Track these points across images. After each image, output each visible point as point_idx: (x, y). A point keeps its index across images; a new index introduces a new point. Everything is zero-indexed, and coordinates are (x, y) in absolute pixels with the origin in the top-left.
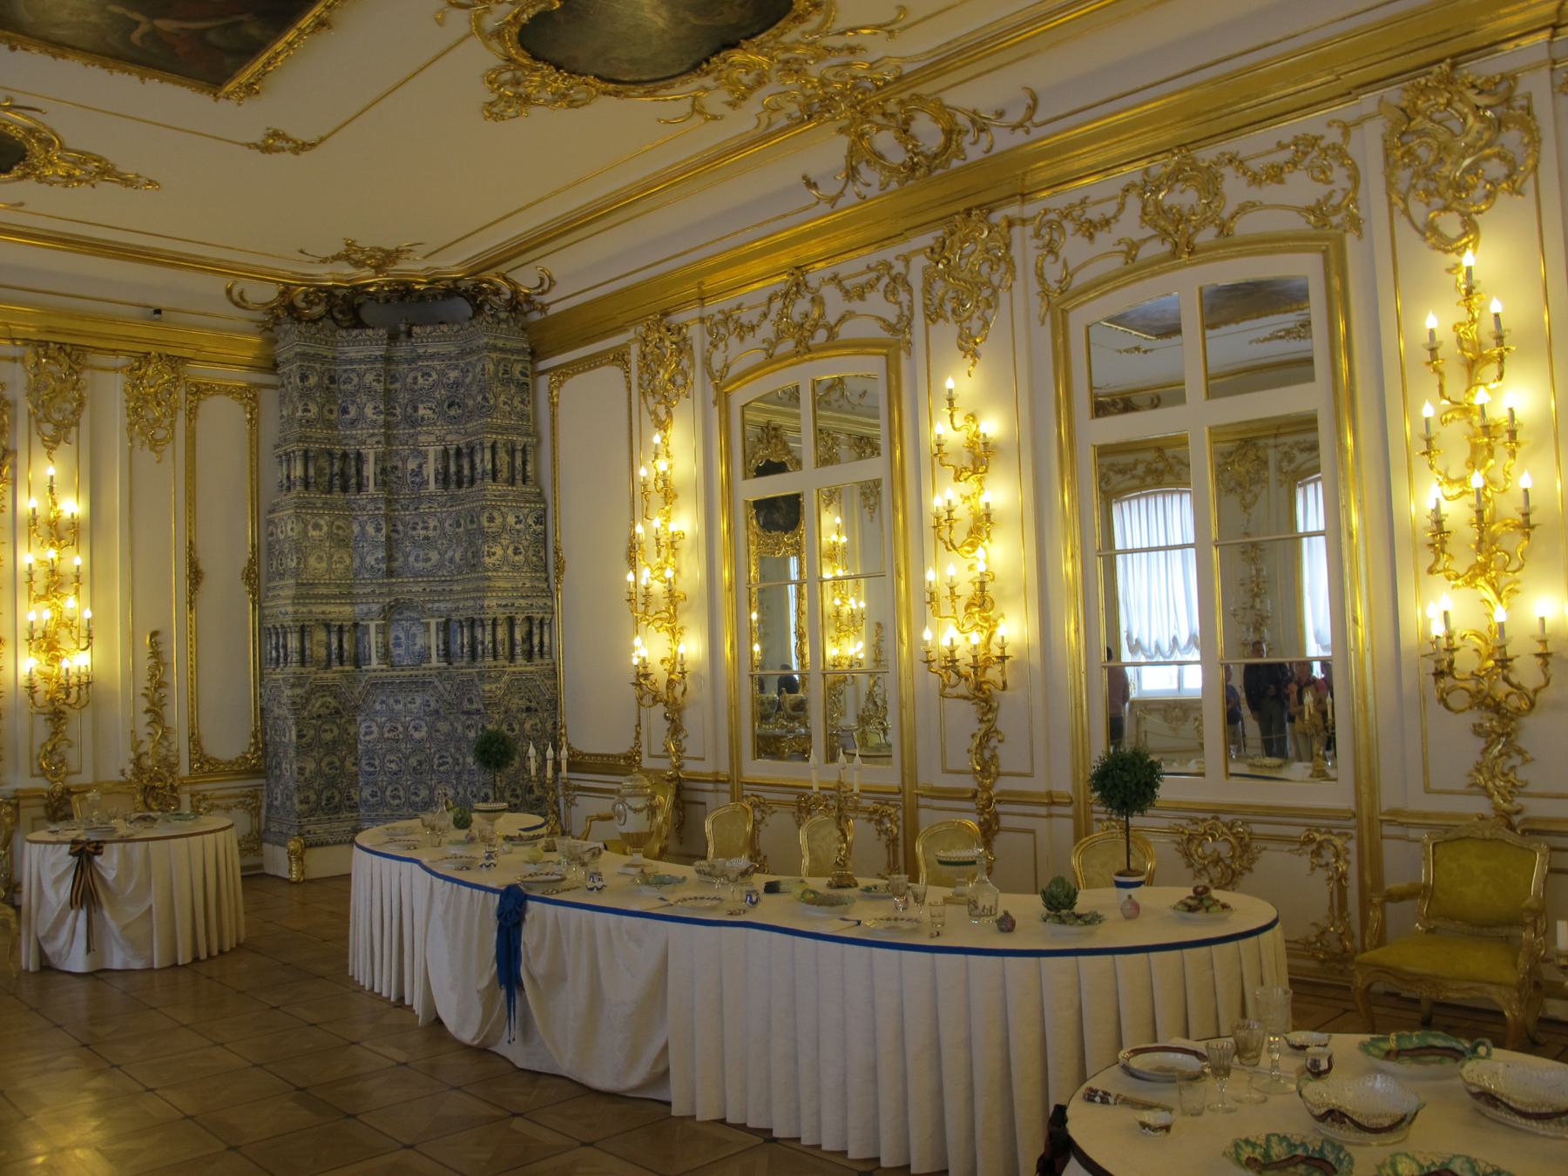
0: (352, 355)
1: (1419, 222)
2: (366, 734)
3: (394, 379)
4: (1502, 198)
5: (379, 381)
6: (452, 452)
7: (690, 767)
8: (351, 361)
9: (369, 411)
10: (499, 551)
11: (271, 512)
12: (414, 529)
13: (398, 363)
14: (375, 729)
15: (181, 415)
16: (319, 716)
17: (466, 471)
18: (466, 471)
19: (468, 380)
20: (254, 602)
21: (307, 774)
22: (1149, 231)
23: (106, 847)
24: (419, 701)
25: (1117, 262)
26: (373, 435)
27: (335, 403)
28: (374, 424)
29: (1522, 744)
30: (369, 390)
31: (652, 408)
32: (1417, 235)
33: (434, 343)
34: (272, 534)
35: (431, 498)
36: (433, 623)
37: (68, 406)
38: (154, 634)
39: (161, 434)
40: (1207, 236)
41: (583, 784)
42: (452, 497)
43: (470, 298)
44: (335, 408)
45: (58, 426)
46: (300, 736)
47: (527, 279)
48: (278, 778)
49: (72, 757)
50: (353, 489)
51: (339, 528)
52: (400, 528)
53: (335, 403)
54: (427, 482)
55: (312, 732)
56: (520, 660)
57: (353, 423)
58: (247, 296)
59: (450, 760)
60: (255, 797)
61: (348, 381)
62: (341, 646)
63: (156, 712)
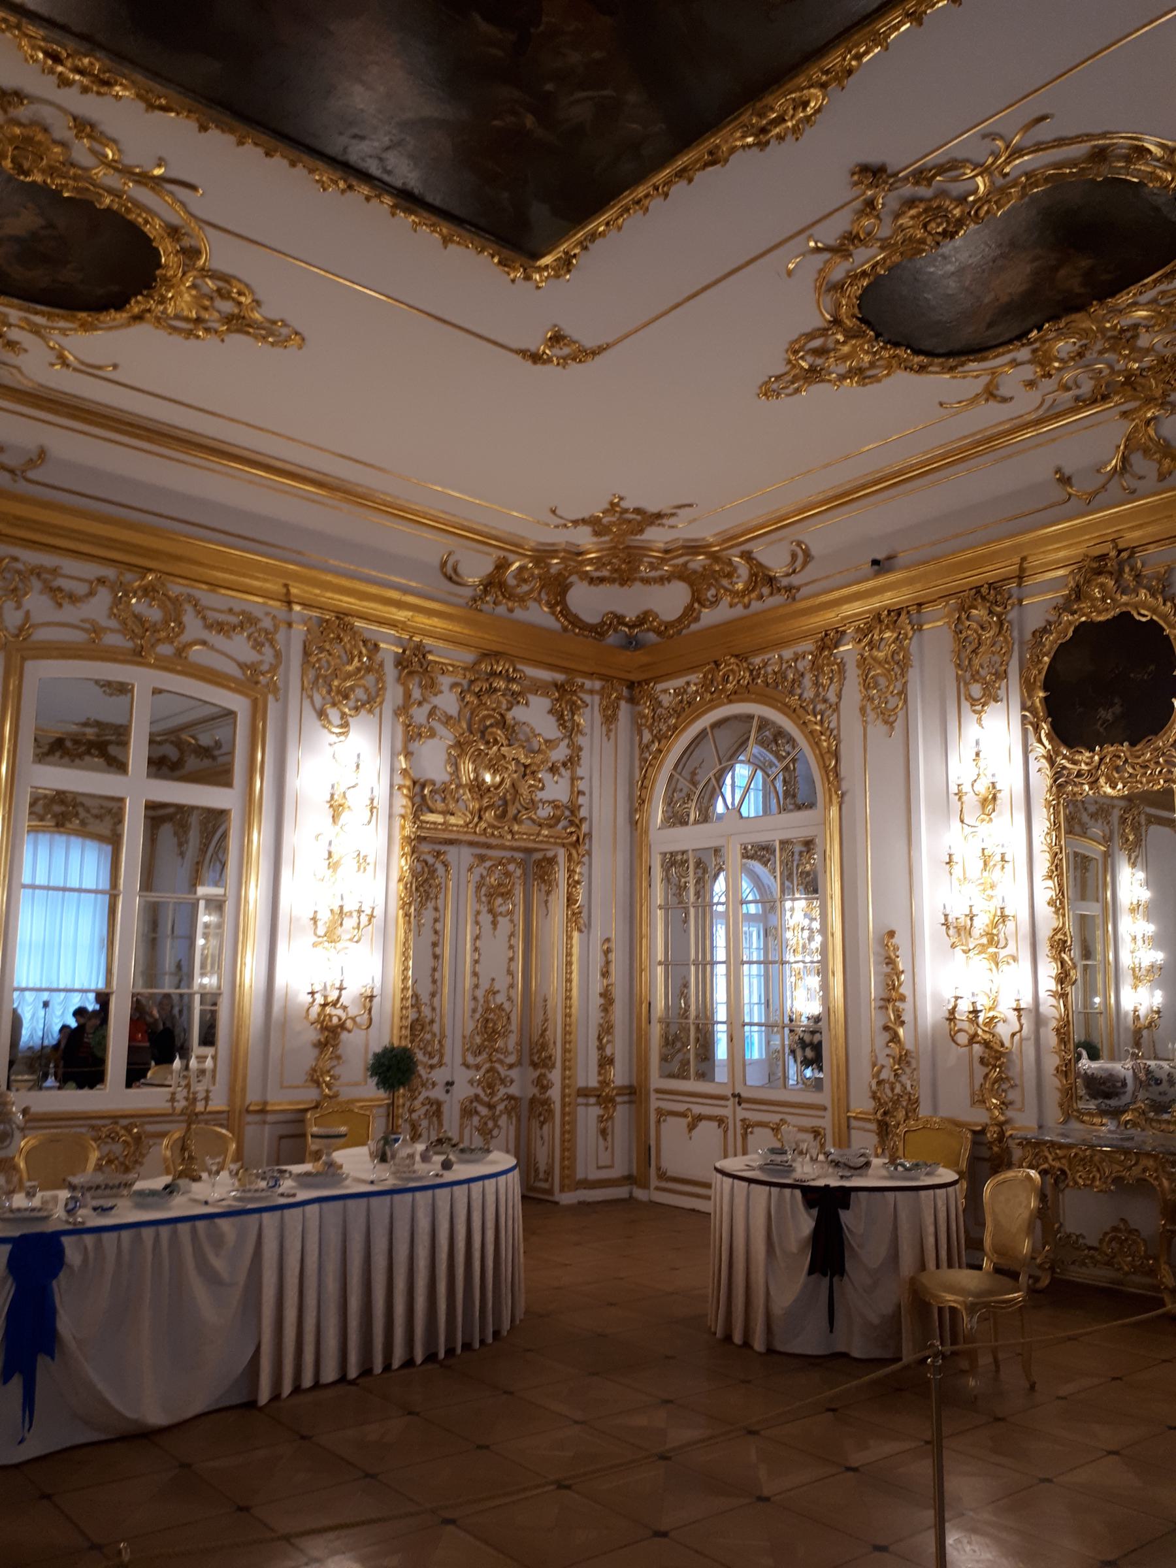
1: (318, 706)
4: (363, 712)
22: (113, 624)
25: (78, 636)
29: (339, 1052)
32: (313, 715)
40: (165, 649)
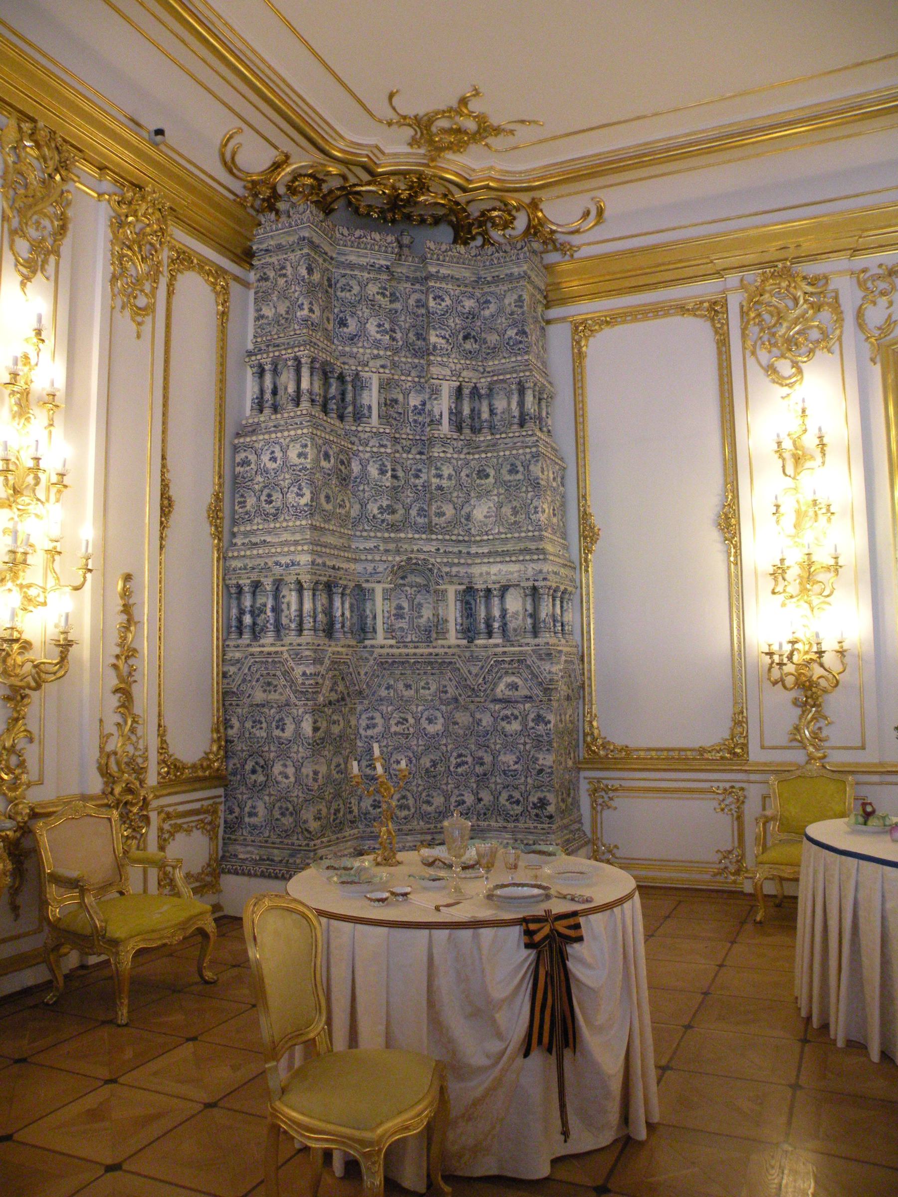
0: (353, 258)
2: (368, 727)
3: (394, 298)
5: (384, 295)
6: (466, 391)
7: (837, 758)
8: (352, 266)
9: (372, 327)
10: (545, 506)
11: (238, 435)
12: (417, 476)
13: (399, 281)
14: (379, 720)
15: (163, 281)
16: (330, 703)
17: (485, 415)
18: (485, 415)
19: (487, 313)
20: (218, 550)
21: (320, 781)
23: (582, 920)
24: (433, 687)
26: (377, 357)
27: (332, 312)
28: (377, 344)
30: (372, 304)
31: (764, 362)
33: (449, 263)
34: (245, 462)
35: (445, 442)
36: (452, 591)
37: (46, 222)
38: (128, 578)
39: (142, 301)
41: (625, 784)
42: (469, 443)
43: (465, 224)
44: (331, 317)
45: (36, 246)
46: (316, 729)
47: (560, 212)
48: (258, 789)
49: (31, 754)
50: (351, 419)
51: (342, 463)
52: (400, 474)
53: (332, 312)
54: (440, 423)
55: (325, 724)
56: (563, 641)
57: (352, 338)
58: (238, 159)
59: (469, 759)
60: (215, 812)
61: (347, 288)
62: (343, 614)
63: (125, 693)
